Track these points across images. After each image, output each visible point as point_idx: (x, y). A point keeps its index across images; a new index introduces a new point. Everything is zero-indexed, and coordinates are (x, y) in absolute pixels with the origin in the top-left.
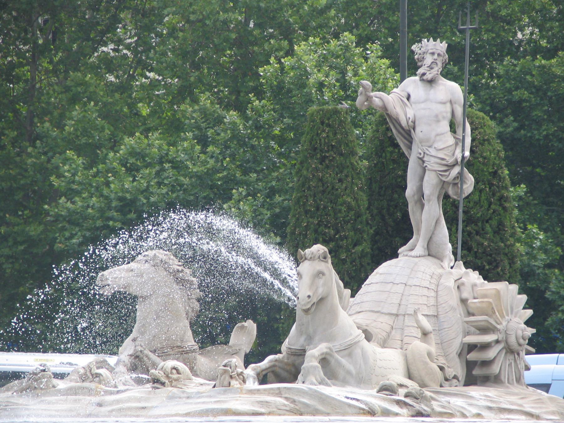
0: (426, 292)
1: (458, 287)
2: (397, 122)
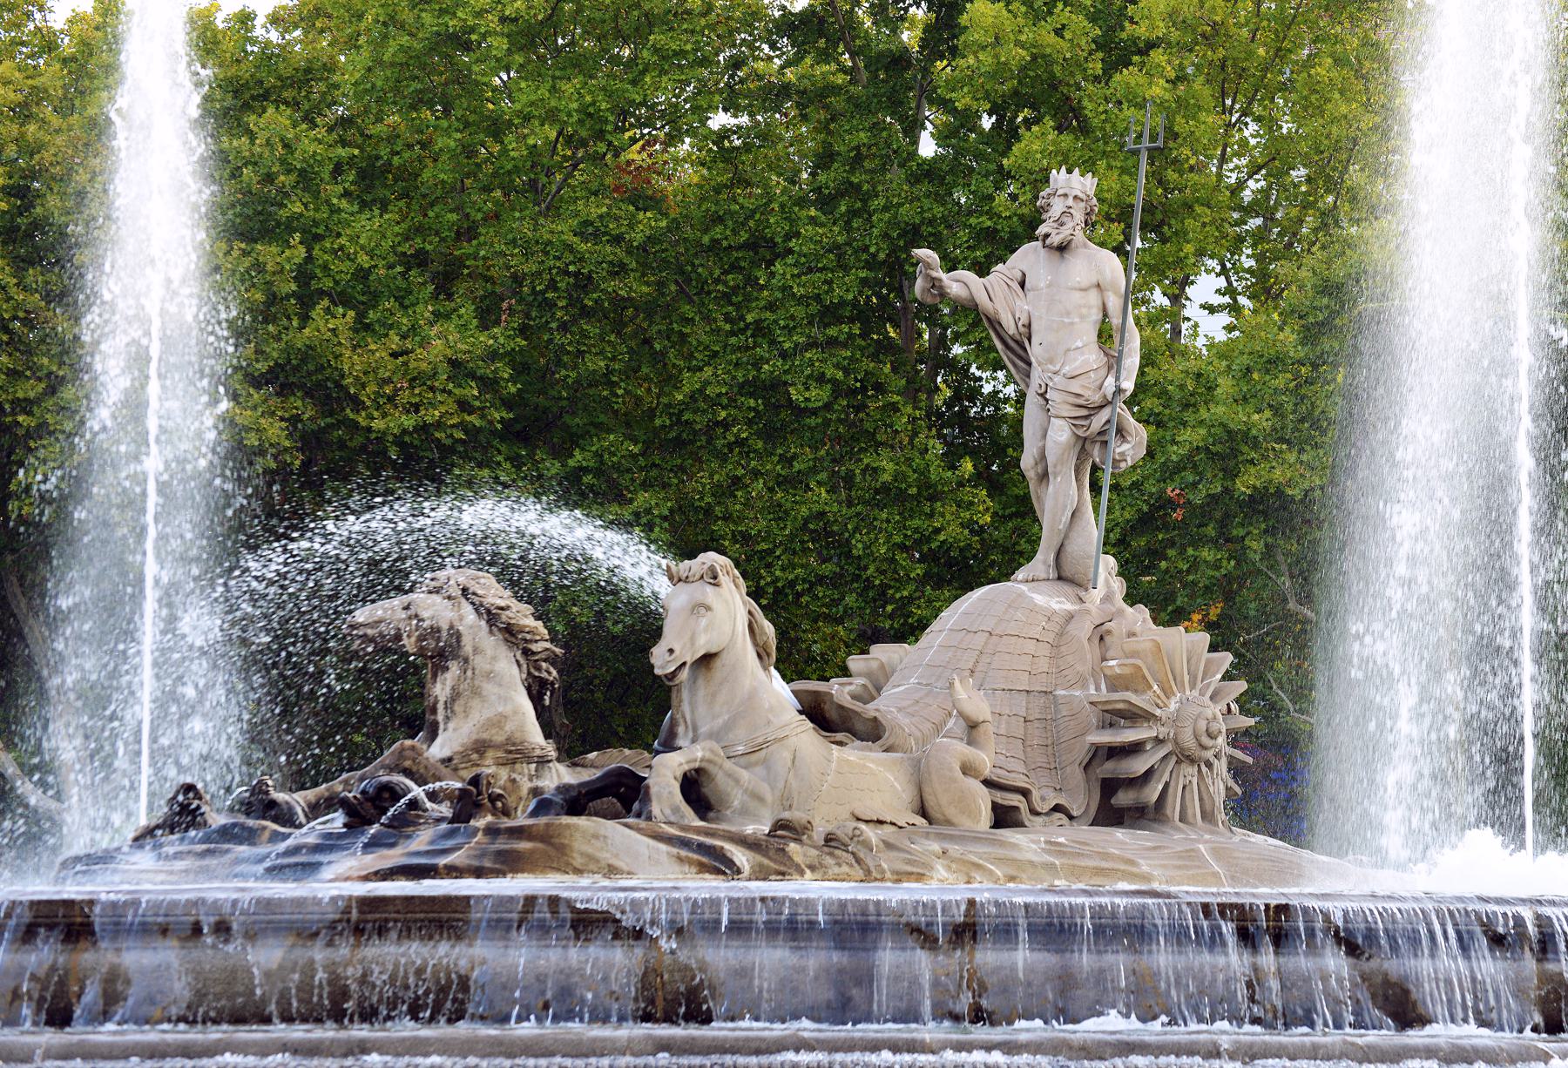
0: (1030, 646)
1: (1102, 638)
2: (995, 324)
